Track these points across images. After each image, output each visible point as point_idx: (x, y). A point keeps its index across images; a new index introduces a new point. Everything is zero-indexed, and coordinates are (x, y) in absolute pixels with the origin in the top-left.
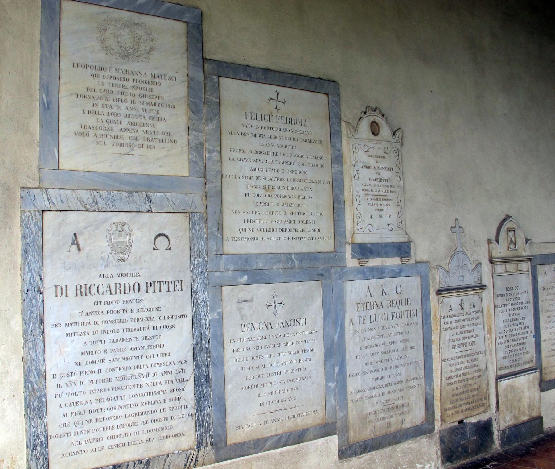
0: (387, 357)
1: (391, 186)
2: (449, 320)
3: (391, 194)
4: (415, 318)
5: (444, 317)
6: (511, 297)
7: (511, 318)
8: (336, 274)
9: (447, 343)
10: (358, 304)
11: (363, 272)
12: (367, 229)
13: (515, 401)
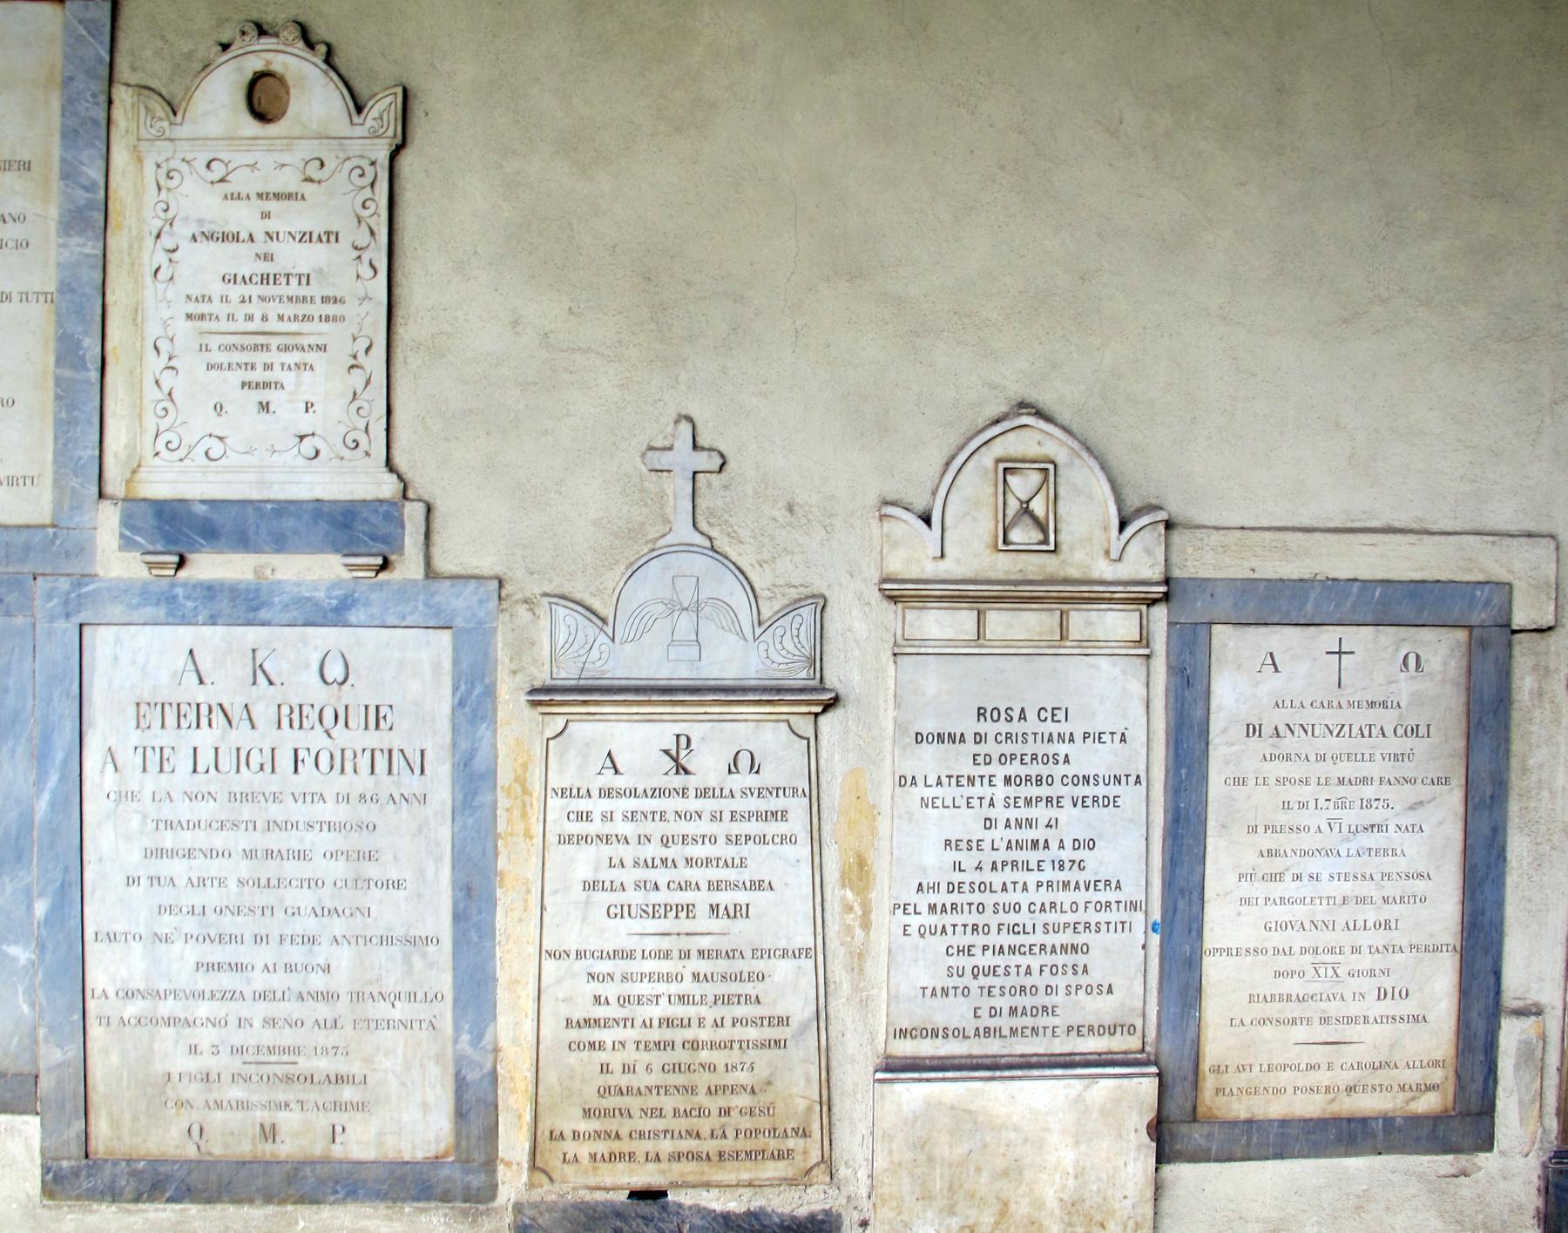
2: (598, 806)
6: (1008, 748)
7: (1000, 834)
13: (978, 1170)
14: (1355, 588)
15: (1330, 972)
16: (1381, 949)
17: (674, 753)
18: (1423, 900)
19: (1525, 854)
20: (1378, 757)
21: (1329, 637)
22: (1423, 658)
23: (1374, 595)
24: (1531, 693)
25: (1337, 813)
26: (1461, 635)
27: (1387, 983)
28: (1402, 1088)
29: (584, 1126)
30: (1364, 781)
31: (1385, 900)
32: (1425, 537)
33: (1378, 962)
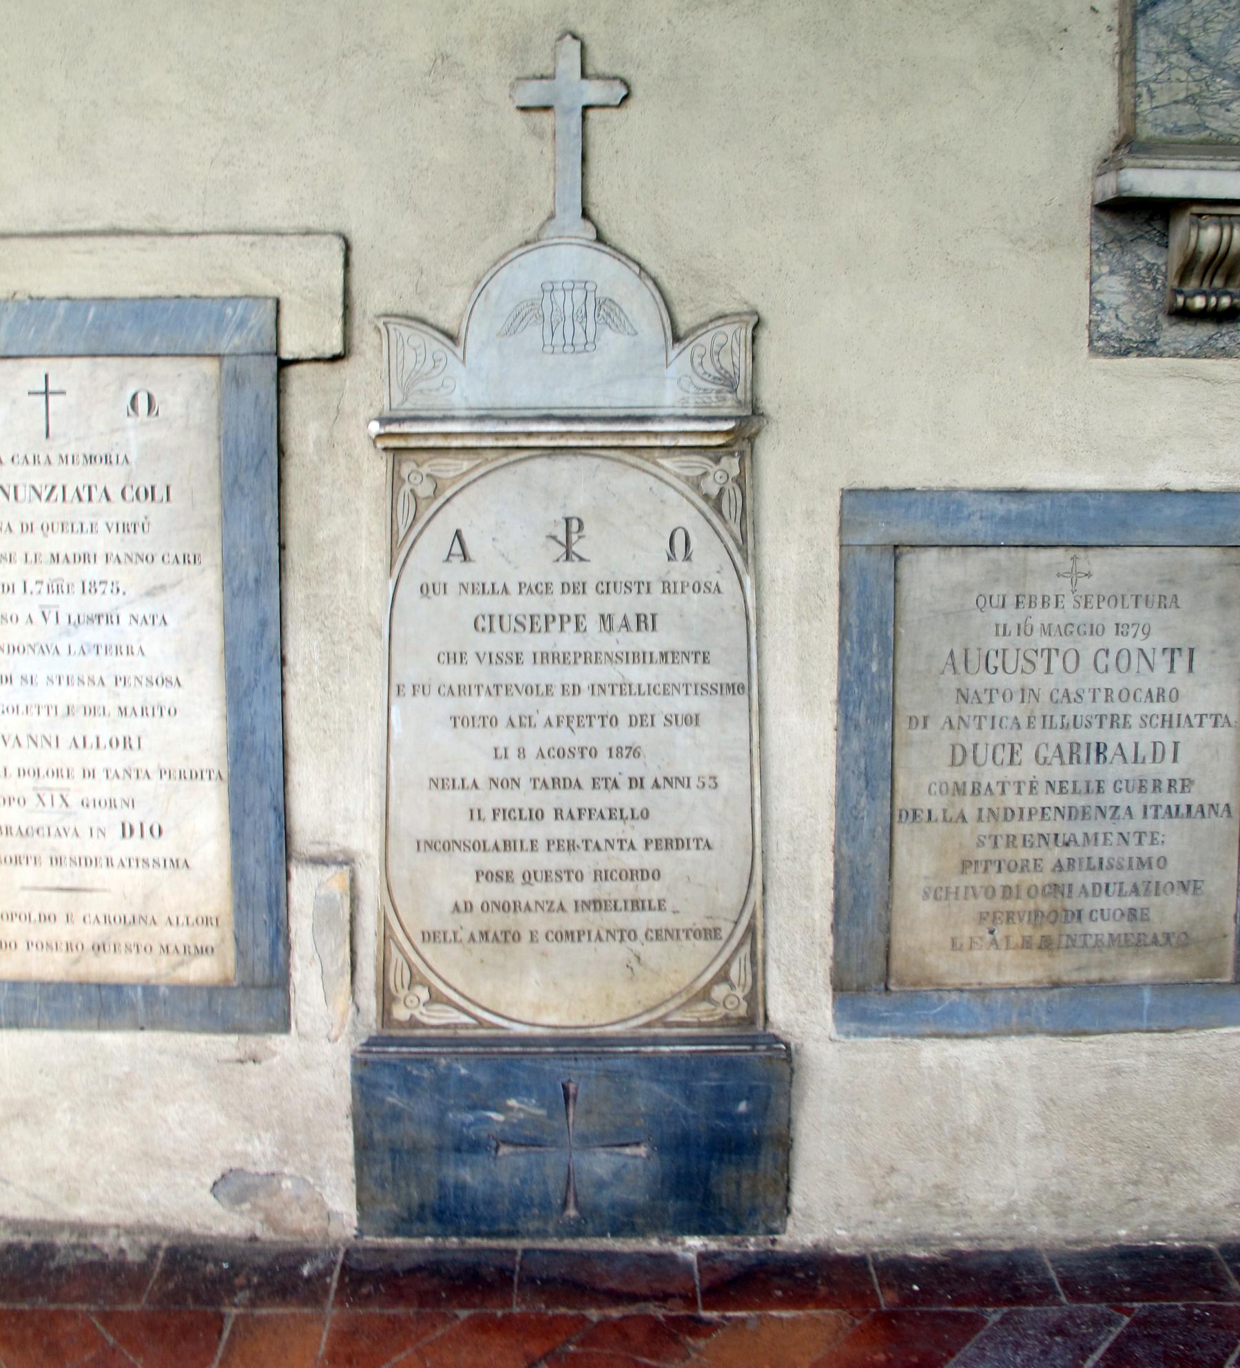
14: (62, 307)
15: (58, 800)
16: (121, 773)
18: (173, 712)
19: (316, 656)
20: (102, 527)
21: (31, 373)
22: (157, 399)
23: (86, 318)
24: (318, 443)
25: (52, 599)
26: (209, 367)
27: (133, 817)
28: (166, 949)
30: (85, 558)
31: (123, 711)
32: (159, 240)
33: (118, 789)
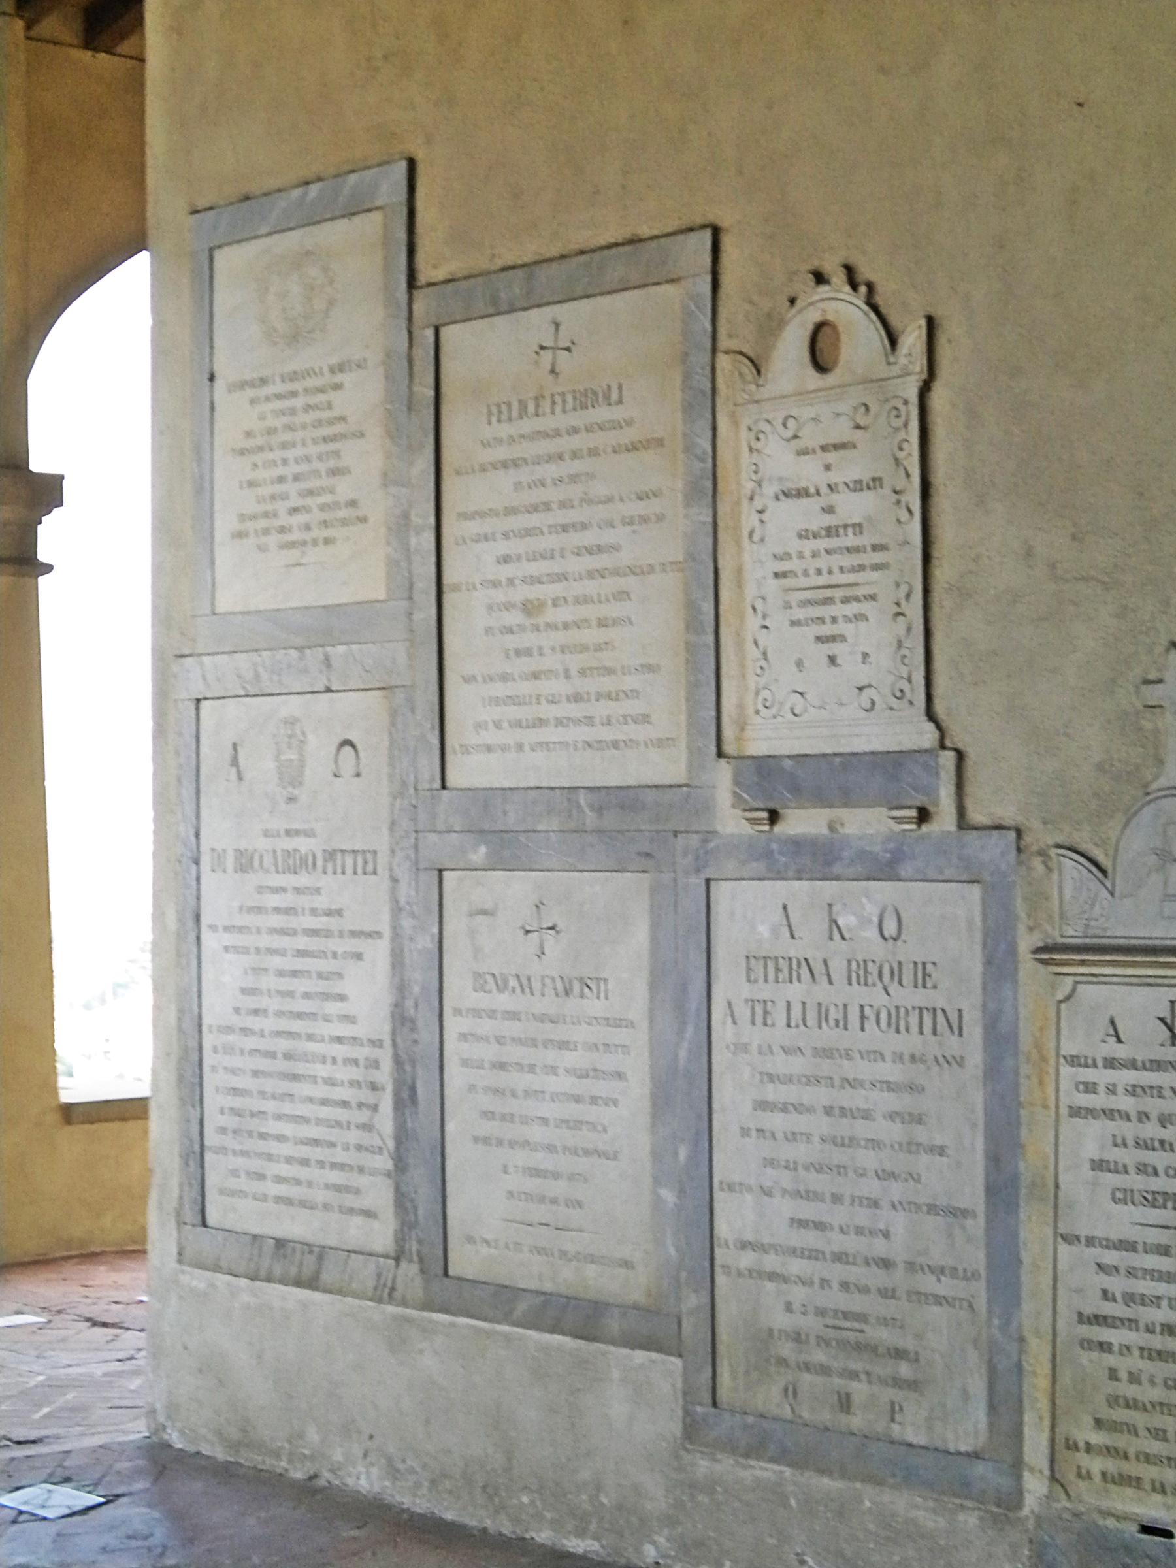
0: (838, 1156)
1: (875, 548)
2: (1103, 1076)
3: (875, 575)
4: (953, 1044)
5: (1073, 1061)
8: (685, 854)
9: (1086, 1172)
10: (753, 961)
11: (768, 855)
12: (787, 707)
17: (1169, 1021)
29: (1098, 1438)
